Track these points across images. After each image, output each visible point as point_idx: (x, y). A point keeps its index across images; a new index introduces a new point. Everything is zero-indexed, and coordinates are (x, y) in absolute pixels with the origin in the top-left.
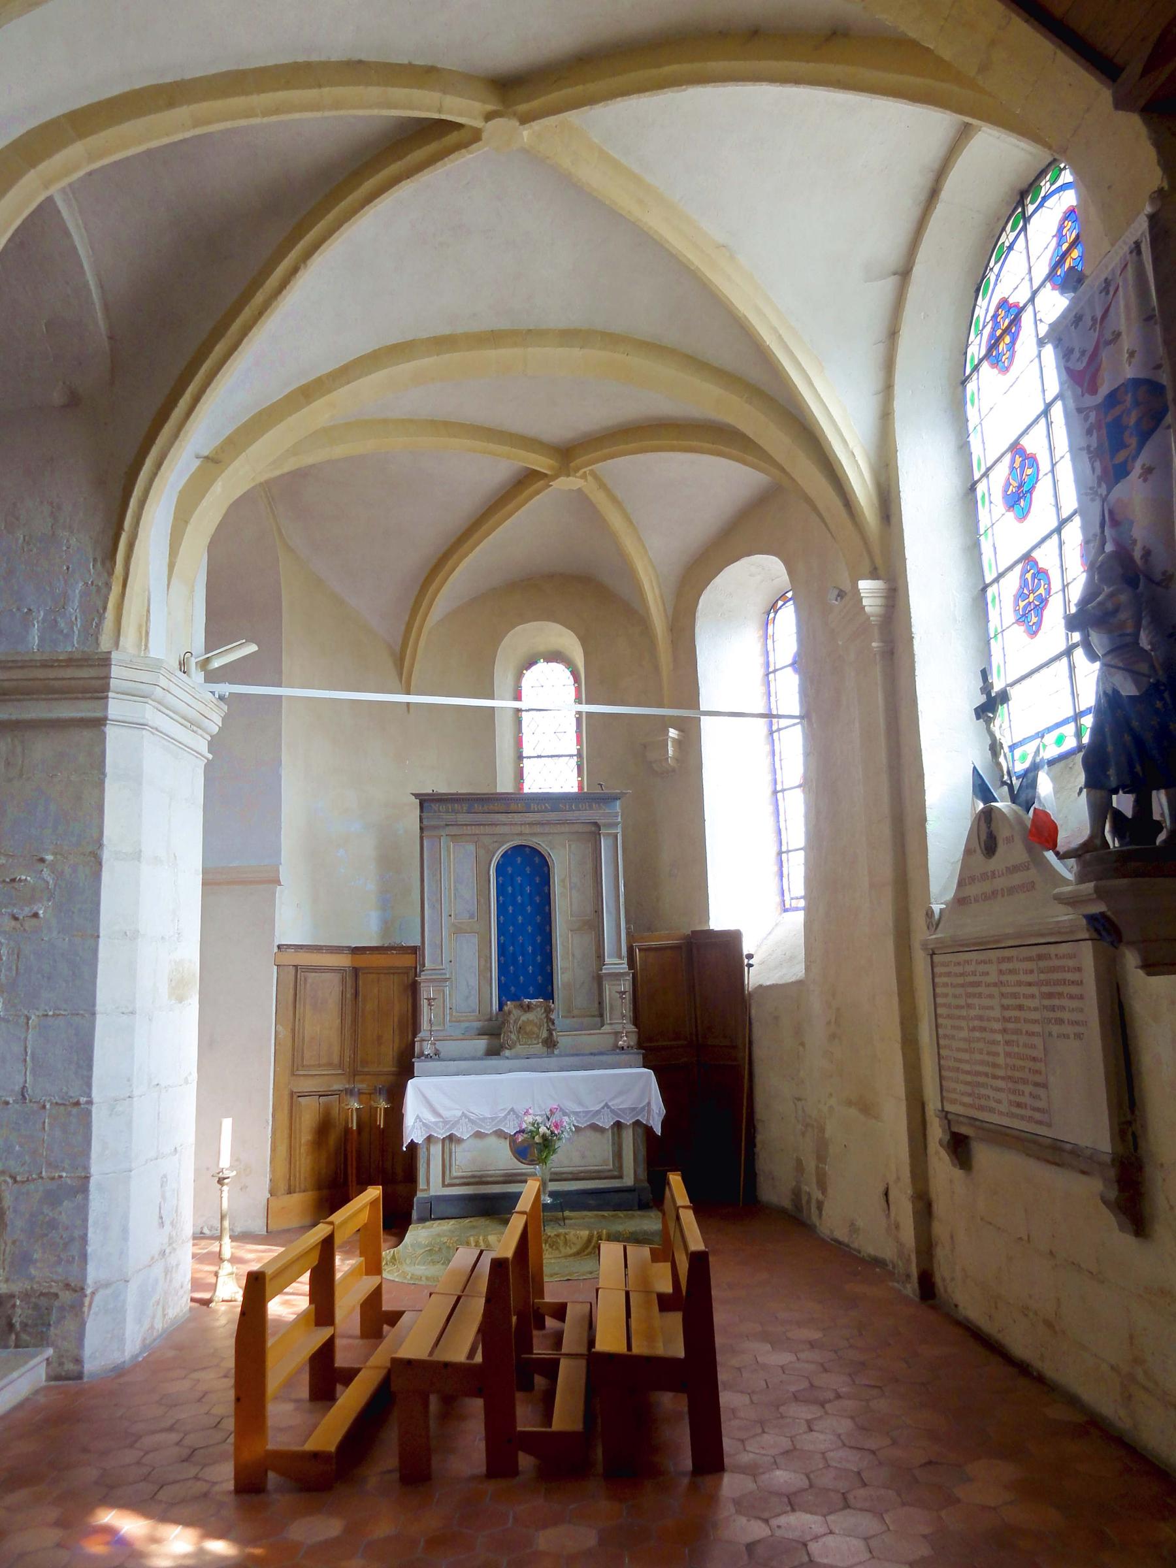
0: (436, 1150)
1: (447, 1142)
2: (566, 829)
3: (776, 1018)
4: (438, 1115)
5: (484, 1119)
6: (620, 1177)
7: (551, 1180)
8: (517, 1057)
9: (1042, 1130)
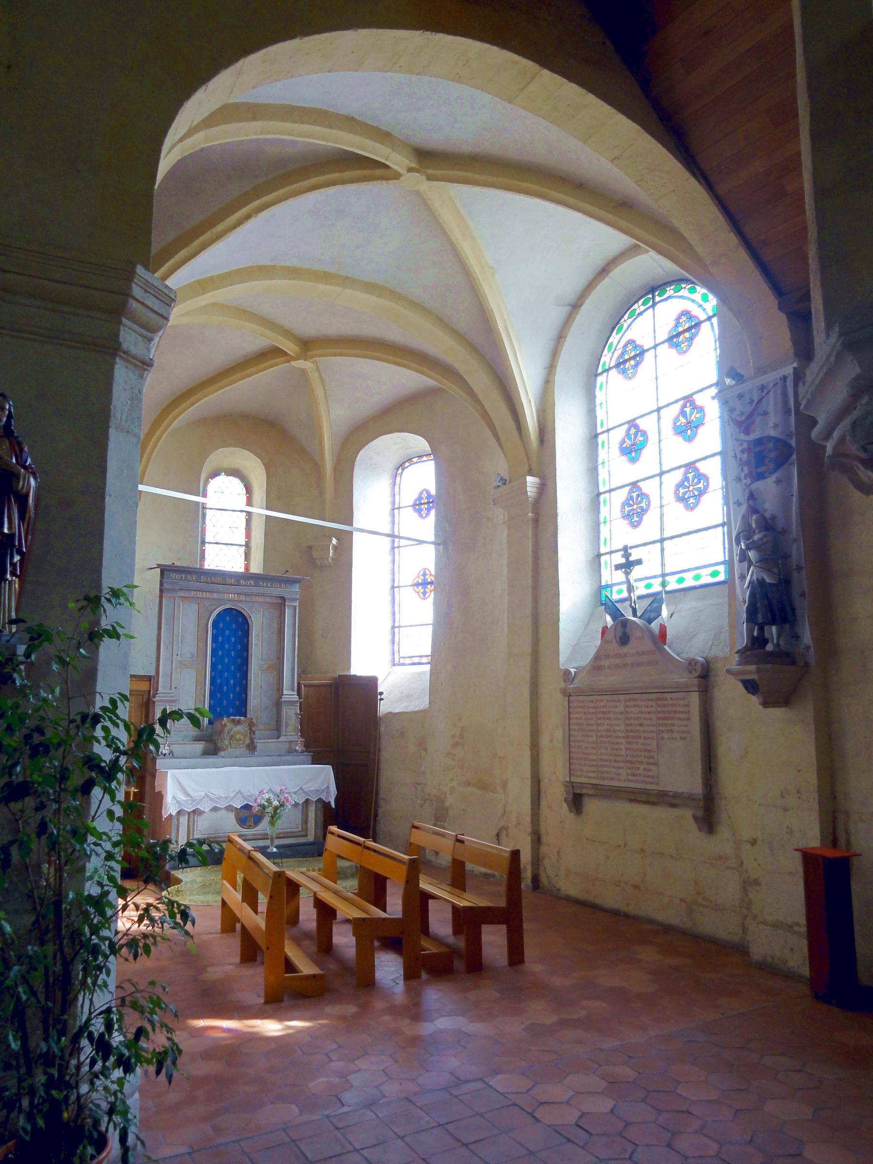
0: (184, 820)
1: (192, 815)
2: (260, 599)
3: (402, 734)
4: (188, 795)
5: (220, 798)
6: (306, 836)
7: (277, 838)
9: (653, 787)
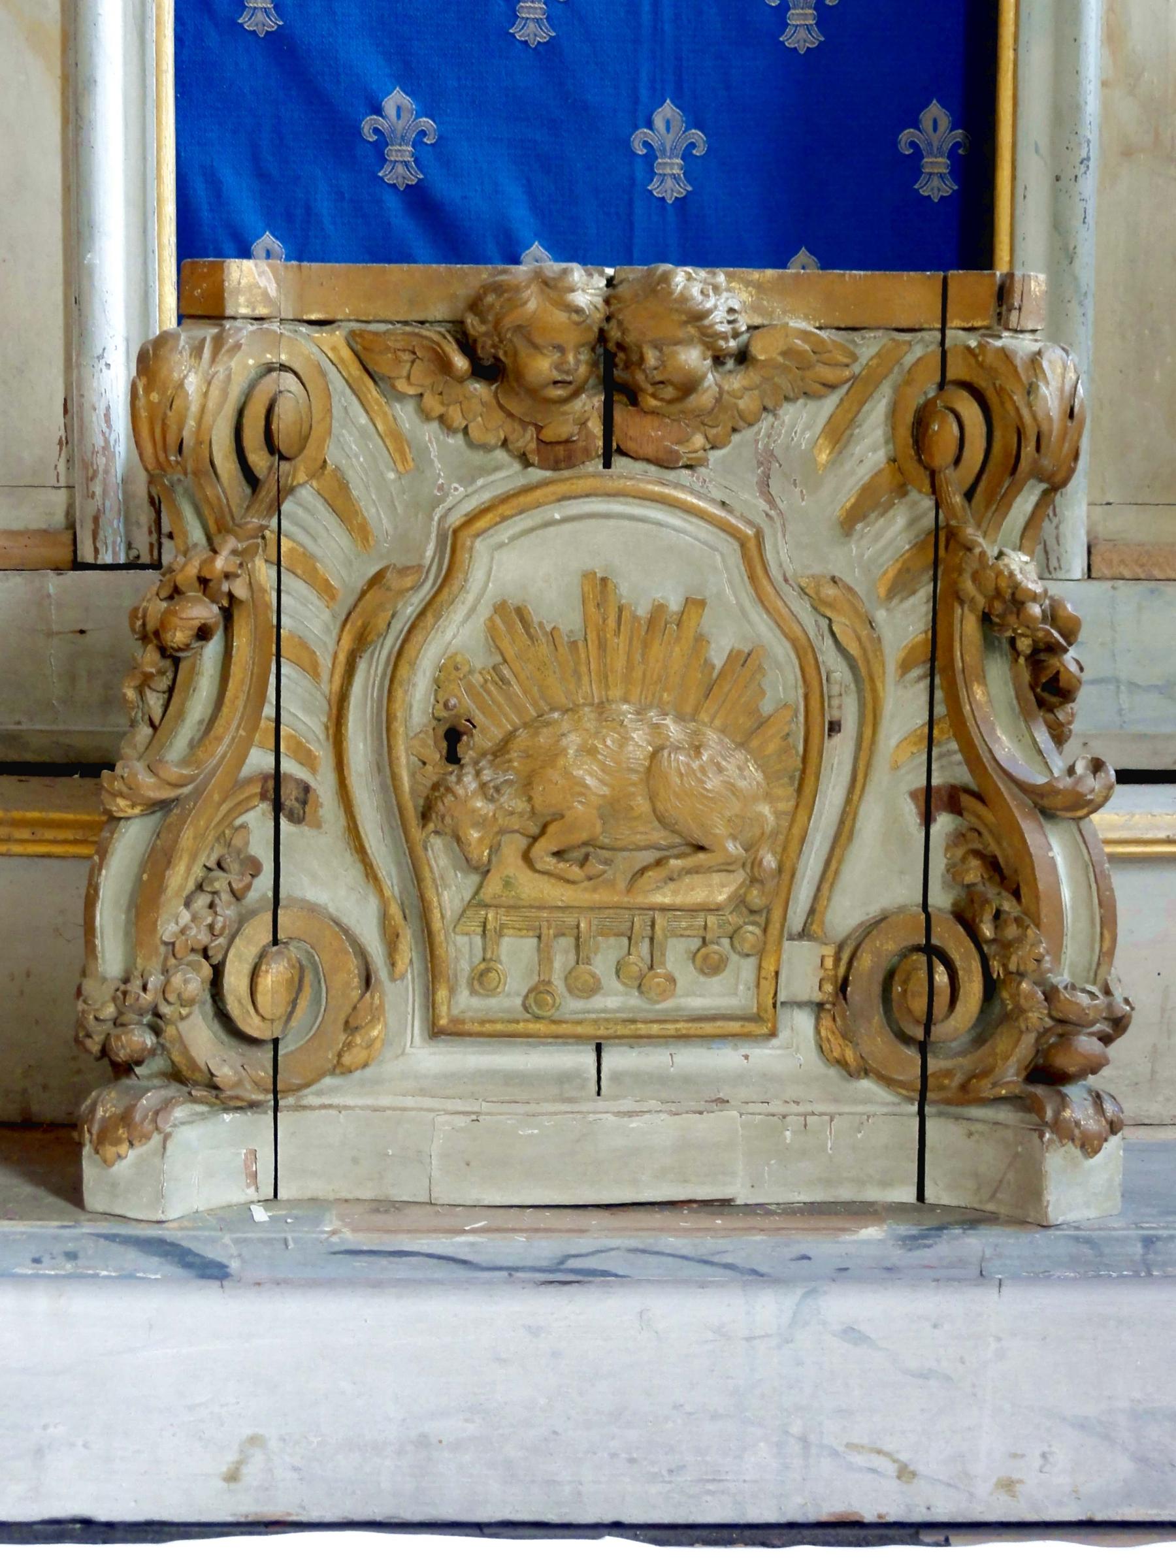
8: (387, 1240)
